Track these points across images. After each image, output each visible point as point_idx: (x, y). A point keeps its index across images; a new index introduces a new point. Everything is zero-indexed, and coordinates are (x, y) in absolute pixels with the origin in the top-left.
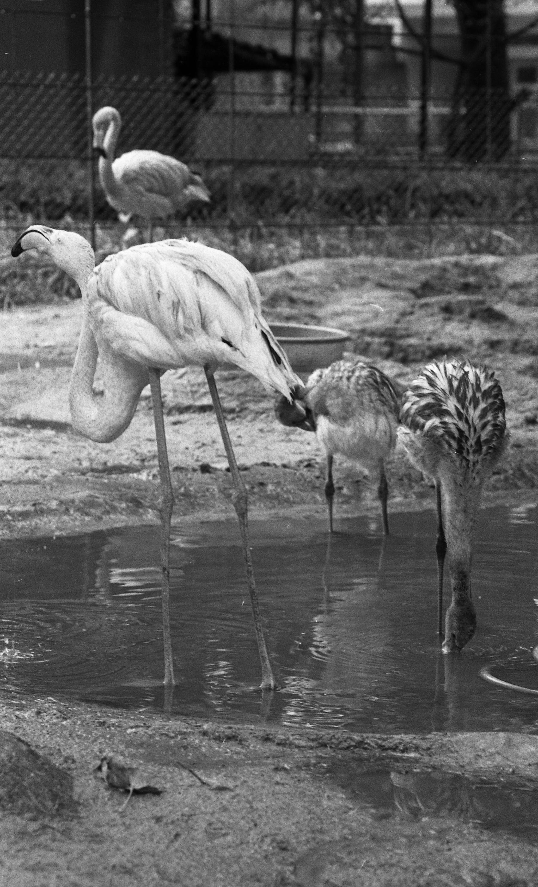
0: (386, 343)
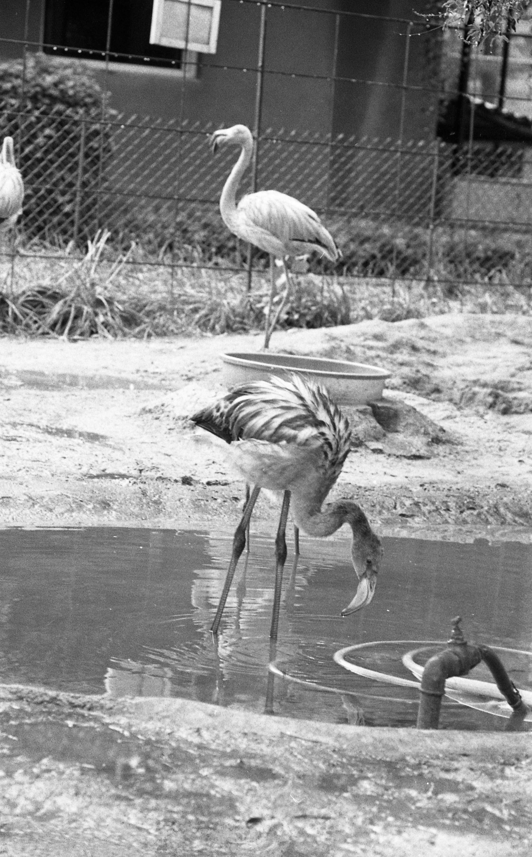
0: (490, 394)
